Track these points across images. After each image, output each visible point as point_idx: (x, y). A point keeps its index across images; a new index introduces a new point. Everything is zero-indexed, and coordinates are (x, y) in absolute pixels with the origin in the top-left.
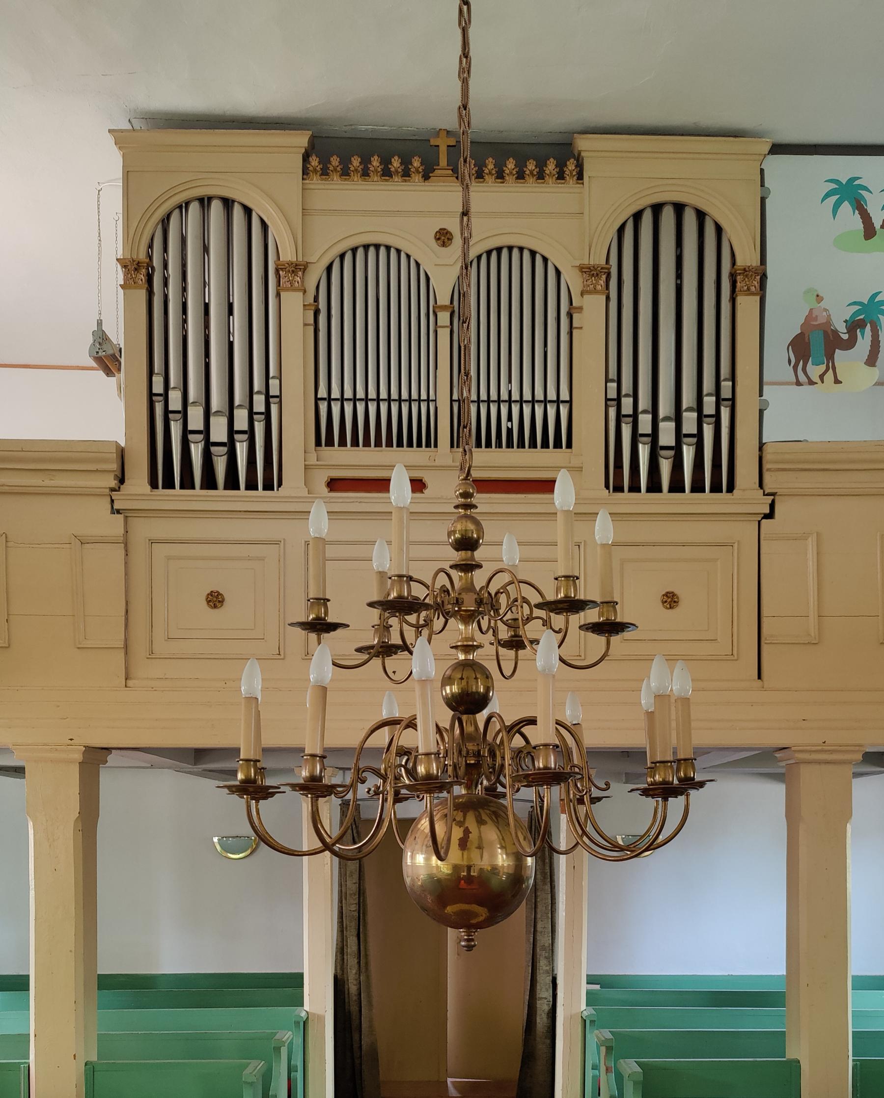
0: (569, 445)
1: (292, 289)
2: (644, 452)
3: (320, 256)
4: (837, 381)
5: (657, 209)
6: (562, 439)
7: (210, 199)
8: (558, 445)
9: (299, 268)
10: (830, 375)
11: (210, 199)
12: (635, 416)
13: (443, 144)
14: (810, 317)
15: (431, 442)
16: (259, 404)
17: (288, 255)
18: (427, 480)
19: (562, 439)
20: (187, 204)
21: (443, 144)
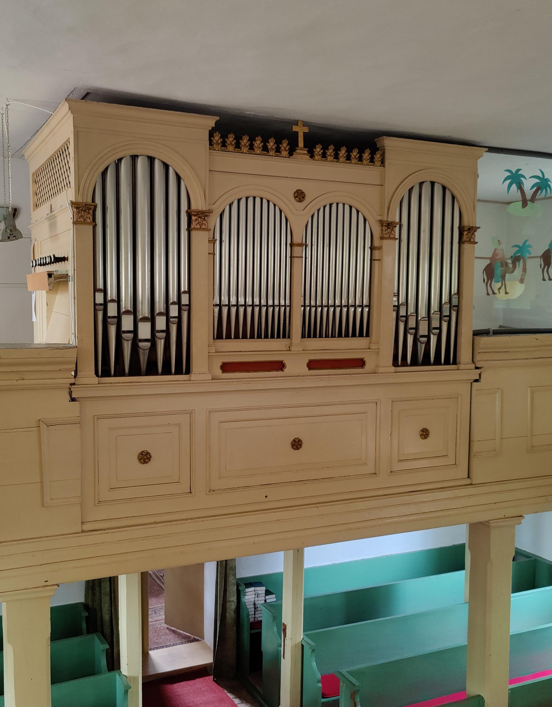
0: (368, 335)
1: (201, 229)
2: (410, 339)
3: (221, 205)
4: (506, 293)
5: (421, 184)
6: (363, 331)
7: (137, 156)
8: (361, 335)
9: (204, 215)
10: (502, 291)
11: (137, 156)
12: (407, 317)
13: (301, 131)
14: (495, 254)
15: (285, 334)
16: (174, 311)
17: (198, 205)
18: (286, 362)
19: (363, 331)
20: (120, 160)
21: (301, 131)
